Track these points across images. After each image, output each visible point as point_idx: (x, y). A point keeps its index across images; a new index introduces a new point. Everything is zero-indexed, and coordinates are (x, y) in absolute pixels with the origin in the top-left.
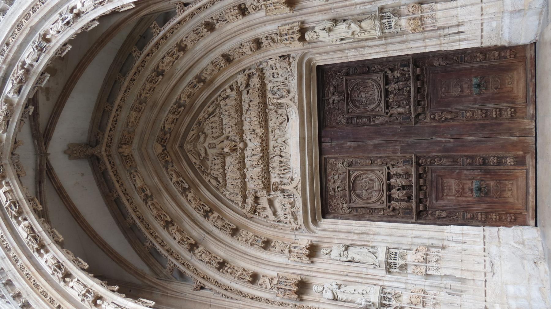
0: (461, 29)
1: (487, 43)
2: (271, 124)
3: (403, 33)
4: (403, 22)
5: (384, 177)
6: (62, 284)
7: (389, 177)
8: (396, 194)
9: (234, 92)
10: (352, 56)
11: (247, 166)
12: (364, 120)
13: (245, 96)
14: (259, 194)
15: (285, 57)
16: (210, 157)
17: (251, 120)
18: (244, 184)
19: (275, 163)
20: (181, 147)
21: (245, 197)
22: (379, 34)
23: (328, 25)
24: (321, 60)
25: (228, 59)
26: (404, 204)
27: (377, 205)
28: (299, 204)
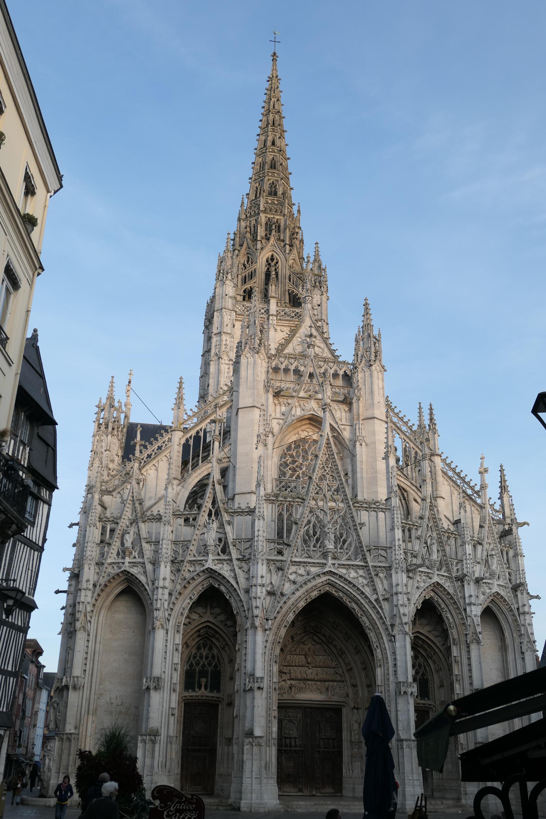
0: (351, 771)
1: (344, 780)
2: (319, 683)
3: (352, 749)
4: (356, 750)
5: (294, 736)
6: (284, 625)
7: (294, 738)
8: (288, 741)
9: (334, 666)
10: (345, 726)
11: (300, 668)
12: (318, 728)
13: (331, 671)
14: (288, 675)
15: (348, 695)
16: (305, 647)
17: (322, 673)
18: (292, 666)
19: (302, 685)
20: (311, 632)
21: (286, 666)
22: (353, 740)
23: (359, 721)
24: (344, 711)
25: (350, 670)
26: (284, 744)
27: (283, 732)
28: (286, 697)
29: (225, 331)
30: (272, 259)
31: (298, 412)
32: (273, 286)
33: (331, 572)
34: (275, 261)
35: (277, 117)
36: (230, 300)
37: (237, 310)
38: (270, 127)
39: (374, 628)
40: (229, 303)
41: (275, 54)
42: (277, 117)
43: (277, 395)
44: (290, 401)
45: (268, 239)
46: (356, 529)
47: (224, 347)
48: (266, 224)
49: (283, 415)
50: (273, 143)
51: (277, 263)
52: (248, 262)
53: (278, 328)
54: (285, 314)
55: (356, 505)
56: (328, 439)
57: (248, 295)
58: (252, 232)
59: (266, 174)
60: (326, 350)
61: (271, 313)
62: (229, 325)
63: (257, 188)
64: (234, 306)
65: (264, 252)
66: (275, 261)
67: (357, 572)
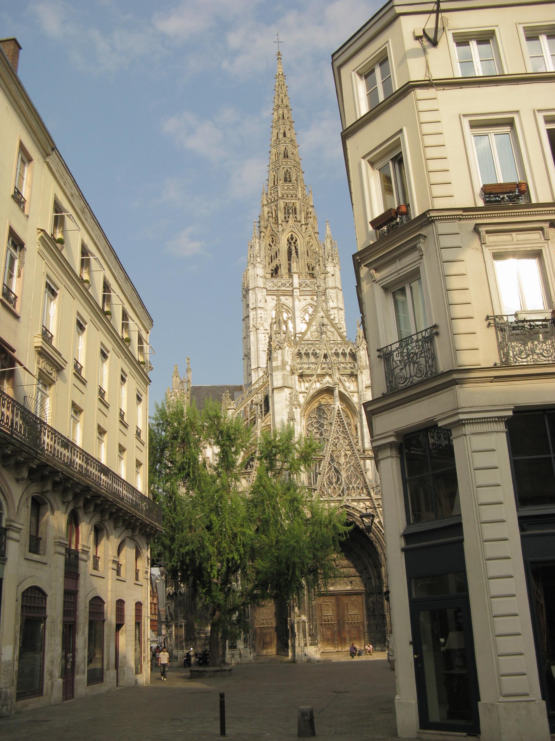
2: (345, 579)
29: (259, 306)
30: (292, 239)
31: (318, 386)
32: (295, 263)
33: (346, 505)
34: (294, 240)
35: (286, 111)
36: (261, 279)
37: (267, 286)
38: (280, 121)
39: (378, 541)
40: (260, 282)
41: (279, 54)
42: (286, 111)
43: (301, 376)
44: (310, 378)
45: (287, 222)
46: (363, 474)
47: (259, 319)
48: (285, 208)
49: (307, 389)
50: (285, 135)
51: (296, 241)
52: (273, 242)
53: (302, 297)
54: (306, 285)
55: (361, 456)
56: (339, 410)
57: (275, 272)
58: (274, 216)
59: (281, 164)
60: (336, 332)
61: (295, 286)
62: (262, 301)
63: (274, 176)
64: (264, 284)
65: (285, 233)
66: (294, 240)
67: (365, 504)
